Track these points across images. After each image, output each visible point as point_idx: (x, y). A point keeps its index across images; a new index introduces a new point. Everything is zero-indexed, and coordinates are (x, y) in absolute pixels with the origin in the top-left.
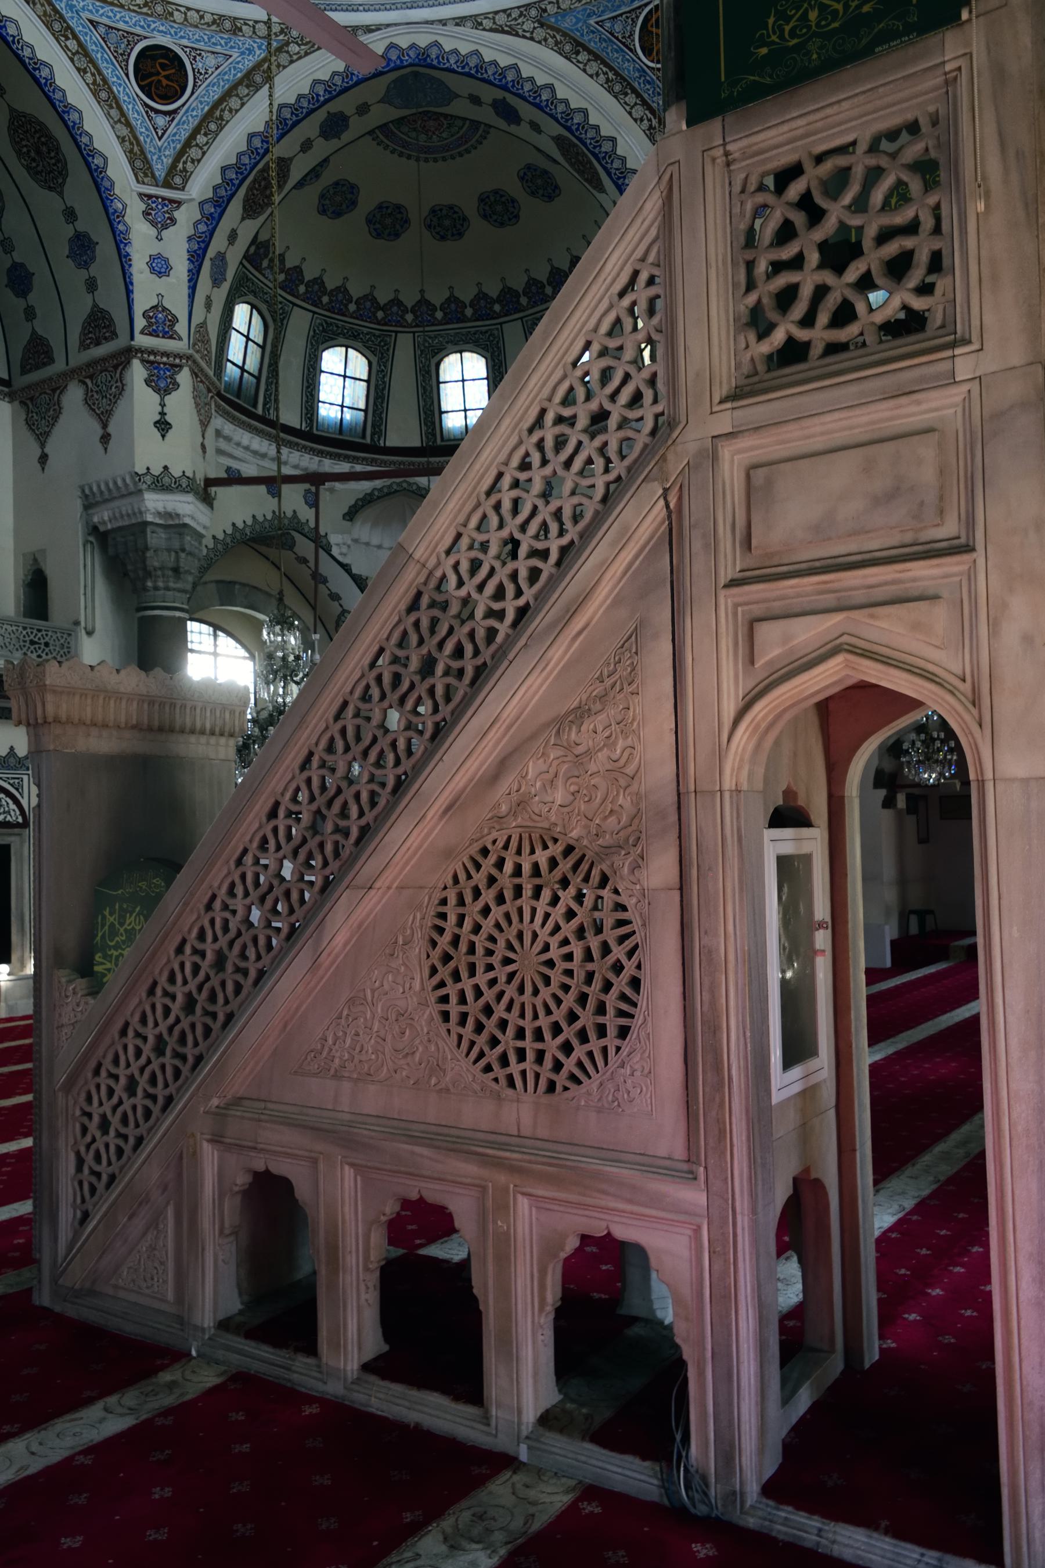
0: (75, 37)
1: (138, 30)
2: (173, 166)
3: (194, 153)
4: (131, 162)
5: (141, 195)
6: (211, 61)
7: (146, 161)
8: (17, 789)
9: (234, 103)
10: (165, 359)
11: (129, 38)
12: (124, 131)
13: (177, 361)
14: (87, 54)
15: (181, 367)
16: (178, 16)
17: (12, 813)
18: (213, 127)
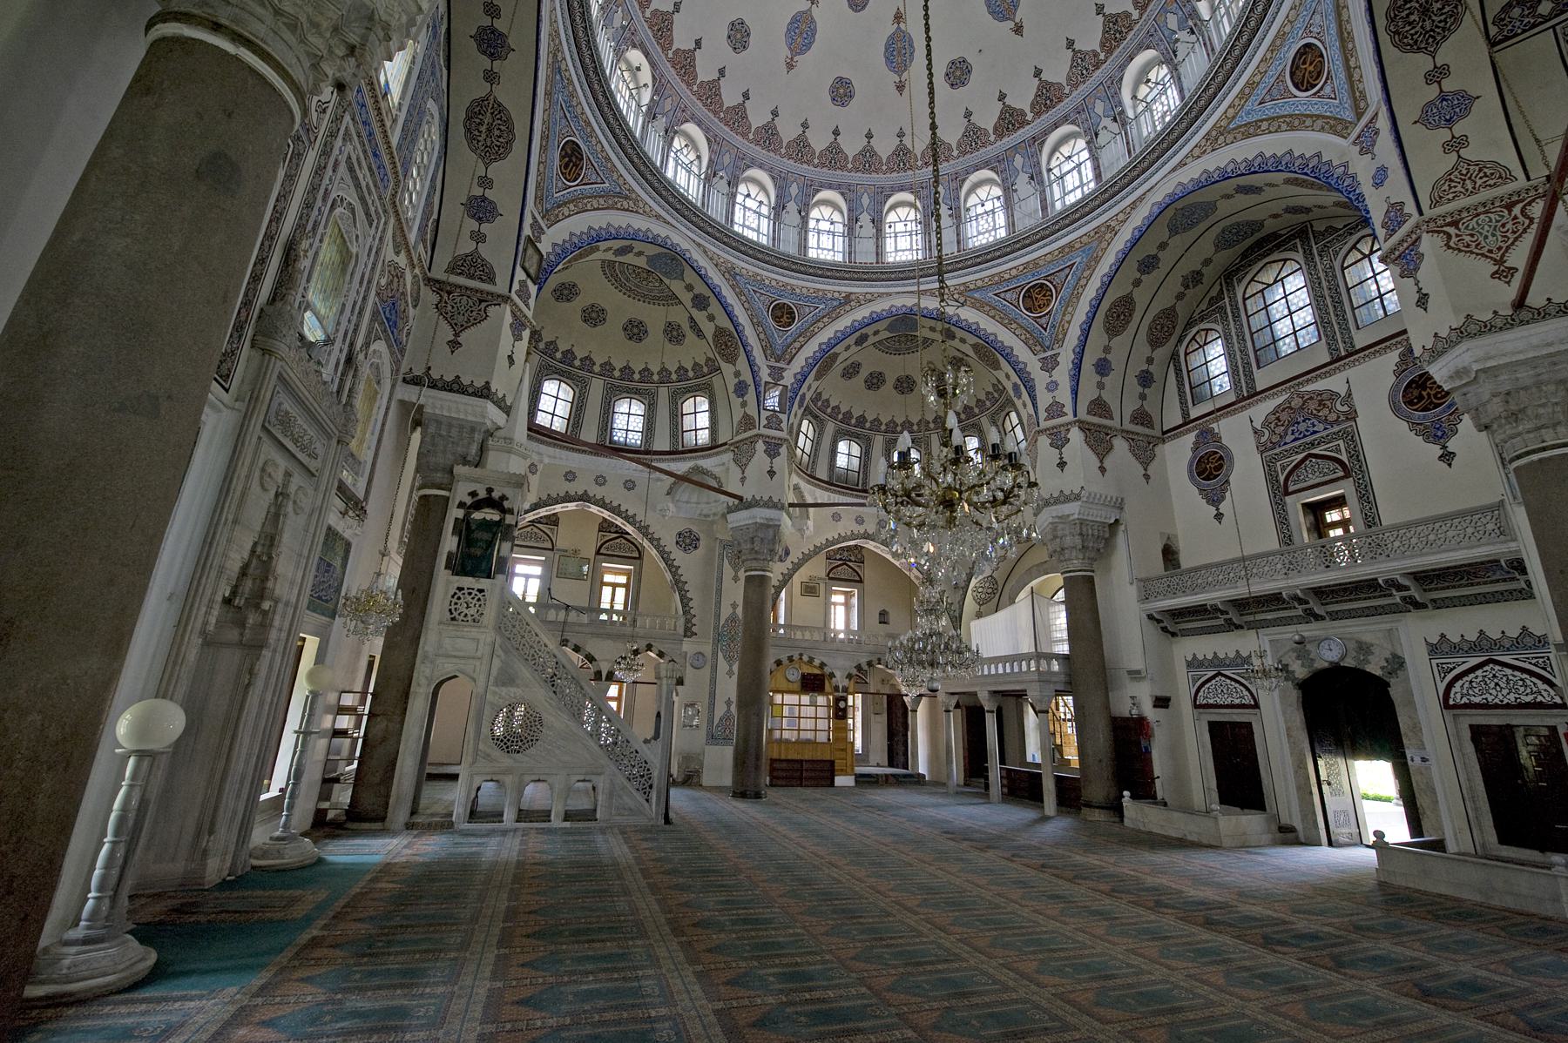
0: (1262, 121)
1: (1280, 69)
2: (1355, 99)
3: (1356, 77)
4: (1336, 133)
5: (1354, 143)
6: (1317, 17)
7: (1340, 121)
8: (1545, 669)
9: (1345, 17)
10: (1405, 245)
11: (1280, 78)
12: (1320, 122)
13: (1414, 236)
14: (1273, 119)
15: (1419, 238)
16: (1287, 29)
17: (1545, 694)
18: (1350, 46)
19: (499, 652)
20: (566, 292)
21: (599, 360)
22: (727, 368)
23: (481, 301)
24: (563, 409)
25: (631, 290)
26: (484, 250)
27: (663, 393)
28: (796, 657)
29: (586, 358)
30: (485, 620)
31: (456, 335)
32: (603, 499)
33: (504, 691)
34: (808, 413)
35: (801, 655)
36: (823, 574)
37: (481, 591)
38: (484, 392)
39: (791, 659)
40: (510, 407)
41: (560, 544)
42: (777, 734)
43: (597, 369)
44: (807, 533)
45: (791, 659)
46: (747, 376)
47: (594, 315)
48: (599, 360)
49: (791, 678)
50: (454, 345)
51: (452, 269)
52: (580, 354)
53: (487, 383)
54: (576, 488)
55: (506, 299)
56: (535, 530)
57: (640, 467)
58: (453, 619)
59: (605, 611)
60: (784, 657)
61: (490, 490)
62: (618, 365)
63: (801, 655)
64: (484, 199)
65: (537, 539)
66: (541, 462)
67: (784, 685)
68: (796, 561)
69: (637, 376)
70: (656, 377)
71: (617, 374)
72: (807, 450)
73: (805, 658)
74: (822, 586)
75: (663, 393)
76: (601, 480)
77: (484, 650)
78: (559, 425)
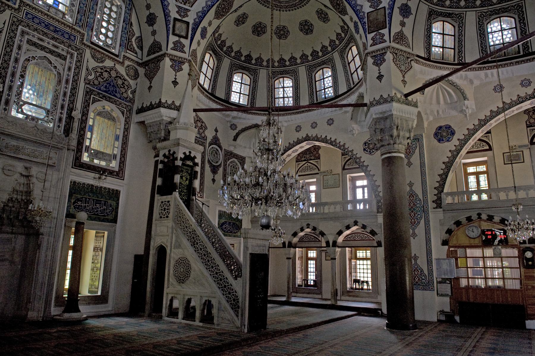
19: (175, 231)
20: (259, 29)
21: (298, 55)
22: (346, 18)
23: (157, 62)
24: (290, 92)
25: (287, 6)
26: (158, 38)
27: (336, 56)
28: (475, 217)
29: (291, 58)
30: (171, 216)
31: (151, 83)
32: (317, 136)
33: (176, 251)
34: (432, 16)
35: (479, 215)
36: (526, 142)
37: (168, 202)
38: (160, 105)
39: (469, 219)
40: (180, 106)
41: (322, 169)
42: (464, 283)
43: (299, 61)
44: (469, 112)
45: (469, 219)
46: (355, 18)
47: (282, 32)
48: (298, 55)
49: (472, 235)
50: (150, 88)
51: (148, 55)
52: (287, 57)
53: (160, 99)
54: (302, 134)
55: (164, 55)
56: (309, 164)
57: (334, 109)
58: (161, 217)
59: (350, 202)
60: (462, 218)
61: (169, 151)
62: (308, 53)
63: (479, 215)
64: (150, 14)
65: (311, 169)
66: (283, 126)
67: (464, 241)
68: (462, 137)
69: (320, 54)
70: (329, 49)
71: (310, 58)
72: (450, 42)
73: (484, 217)
74: (526, 152)
75: (336, 56)
76: (314, 125)
77: (170, 230)
78: (290, 102)
